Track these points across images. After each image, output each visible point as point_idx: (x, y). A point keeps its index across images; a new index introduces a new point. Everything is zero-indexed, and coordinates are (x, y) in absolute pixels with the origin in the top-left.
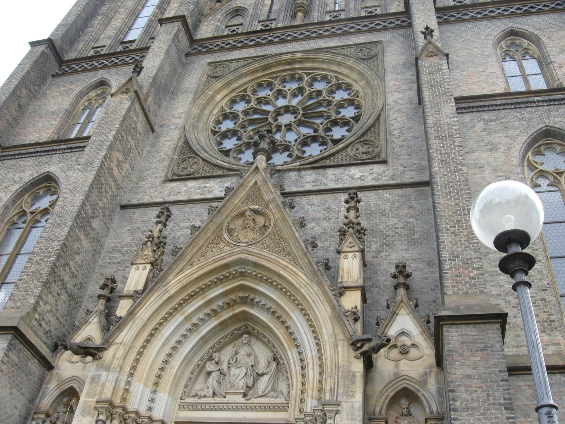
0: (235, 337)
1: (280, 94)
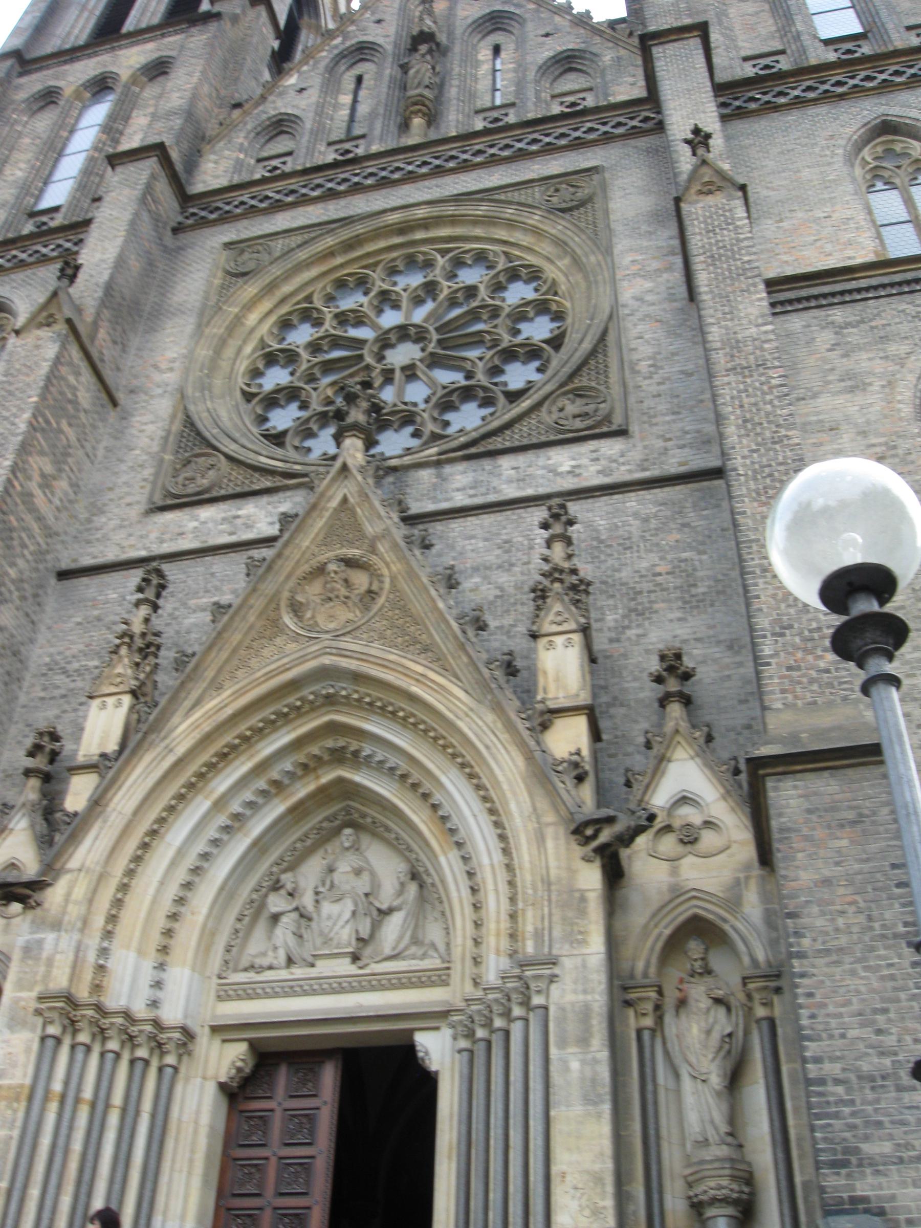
1: (387, 299)
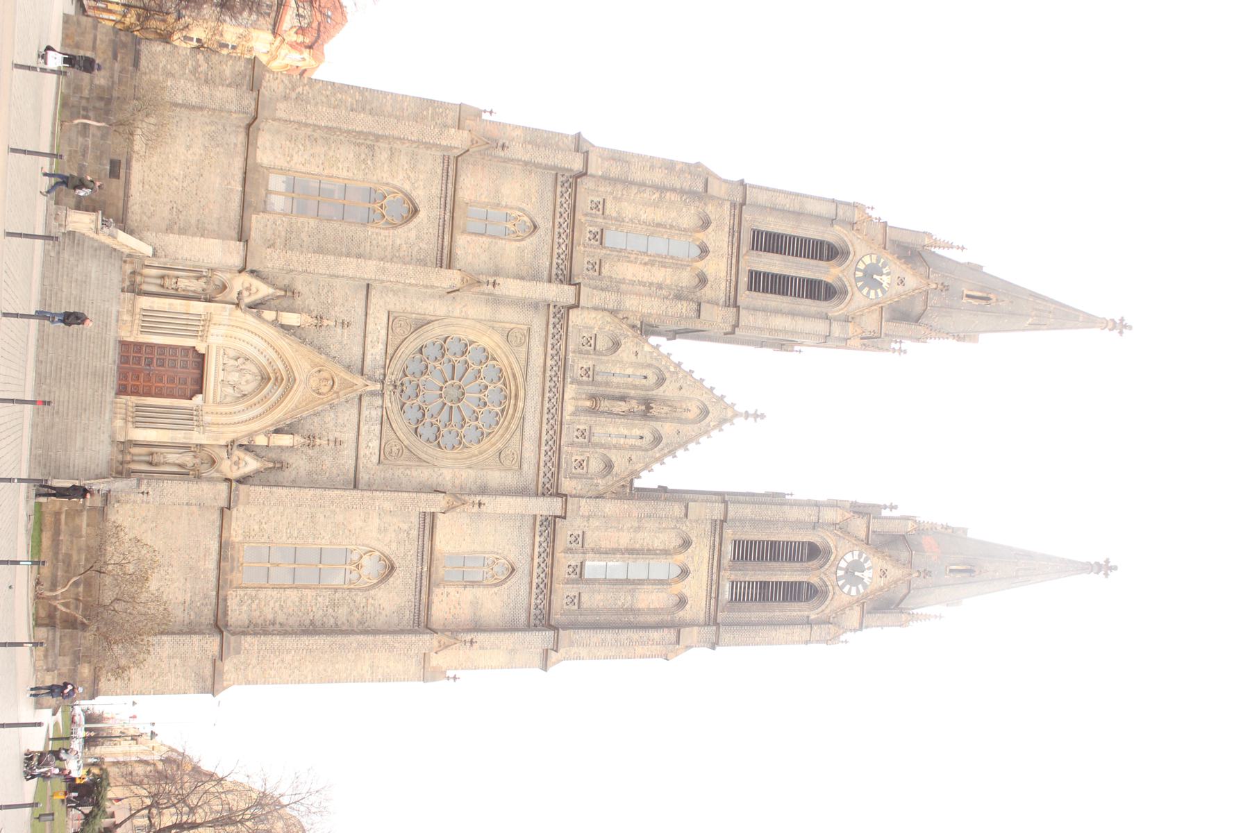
0: (260, 372)
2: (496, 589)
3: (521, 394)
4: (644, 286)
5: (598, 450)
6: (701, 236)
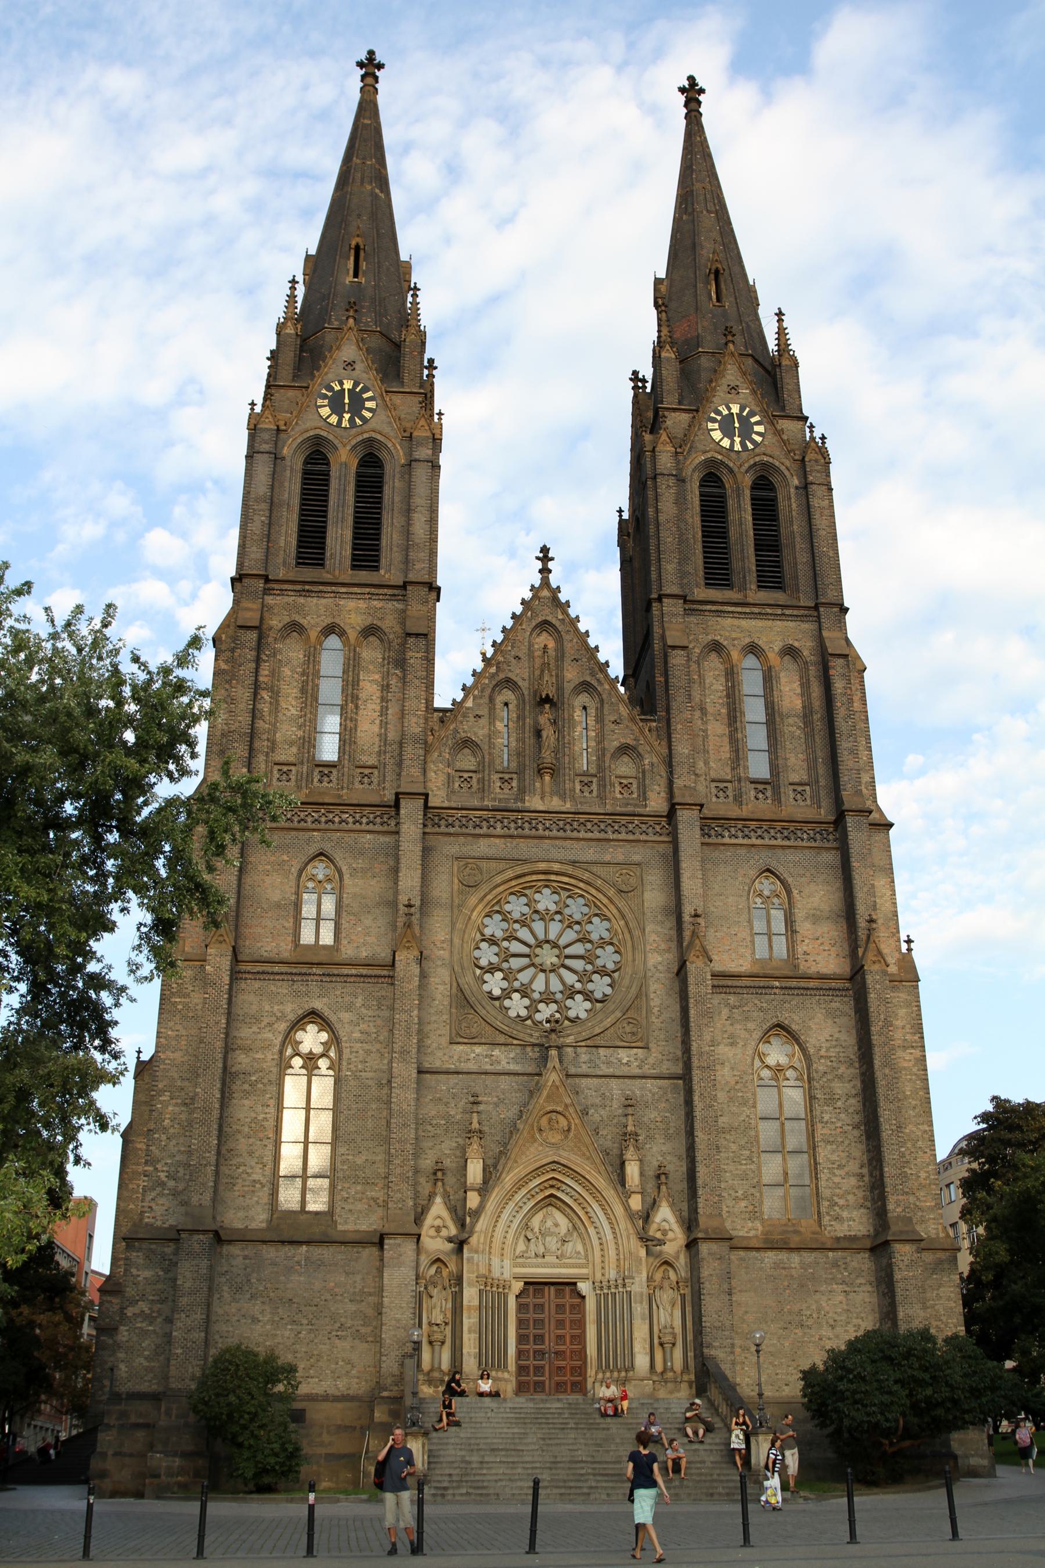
2: (795, 892)
3: (542, 866)
4: (387, 708)
5: (607, 765)
6: (313, 634)
